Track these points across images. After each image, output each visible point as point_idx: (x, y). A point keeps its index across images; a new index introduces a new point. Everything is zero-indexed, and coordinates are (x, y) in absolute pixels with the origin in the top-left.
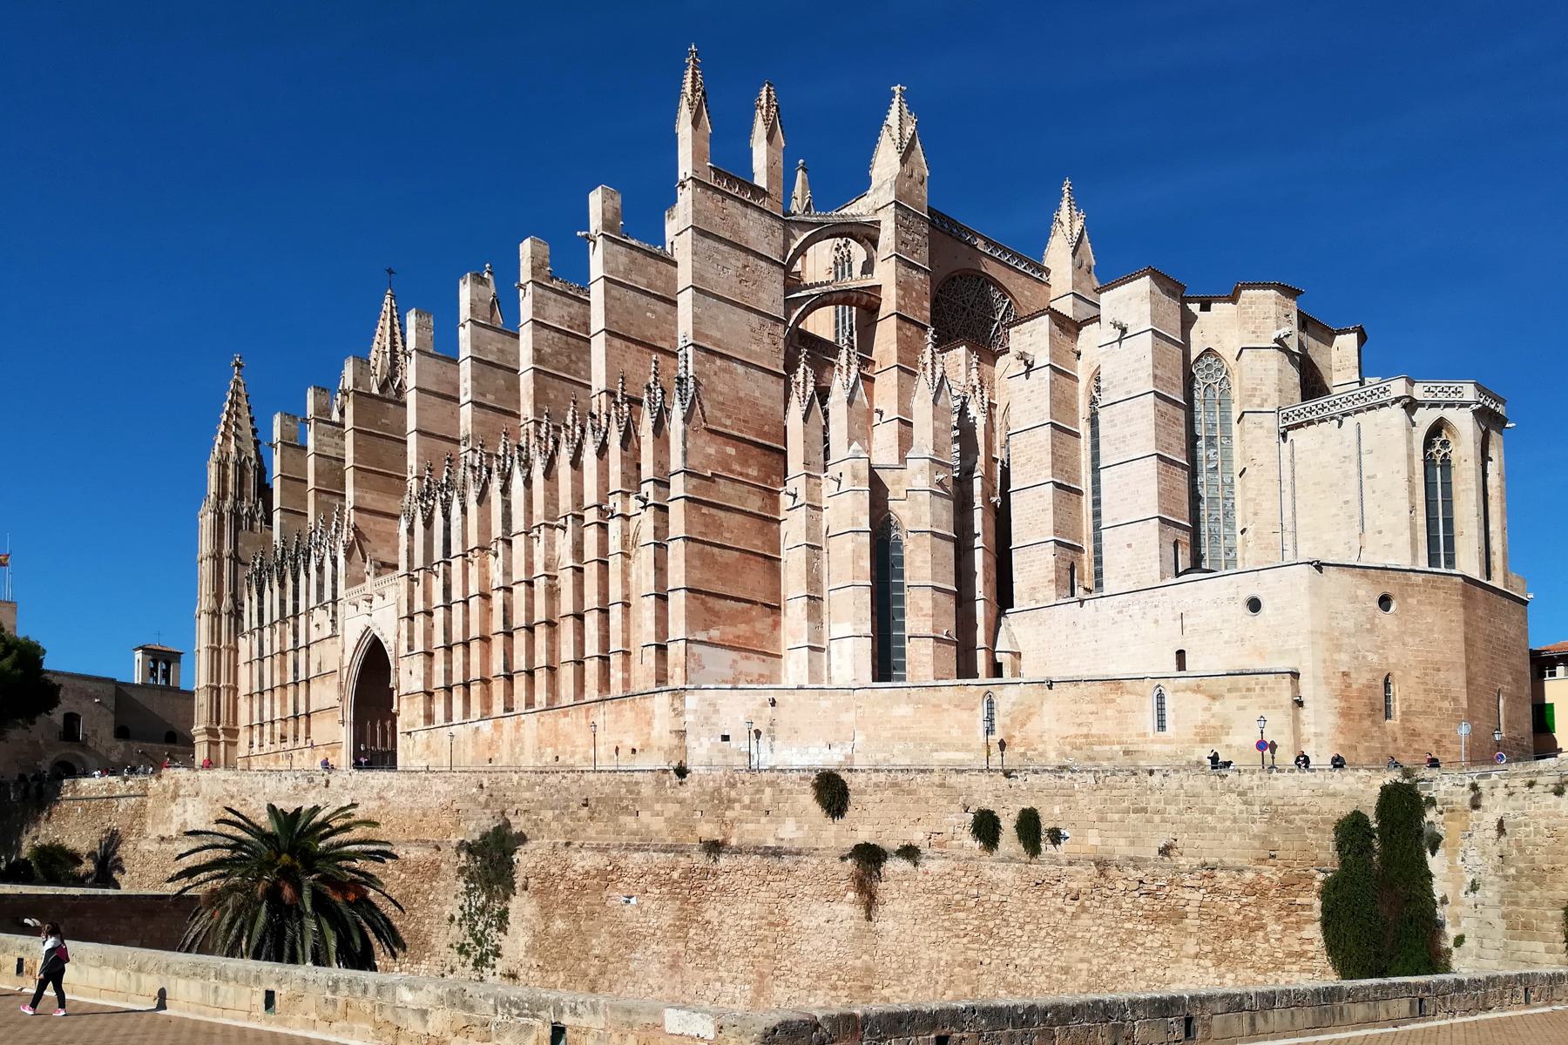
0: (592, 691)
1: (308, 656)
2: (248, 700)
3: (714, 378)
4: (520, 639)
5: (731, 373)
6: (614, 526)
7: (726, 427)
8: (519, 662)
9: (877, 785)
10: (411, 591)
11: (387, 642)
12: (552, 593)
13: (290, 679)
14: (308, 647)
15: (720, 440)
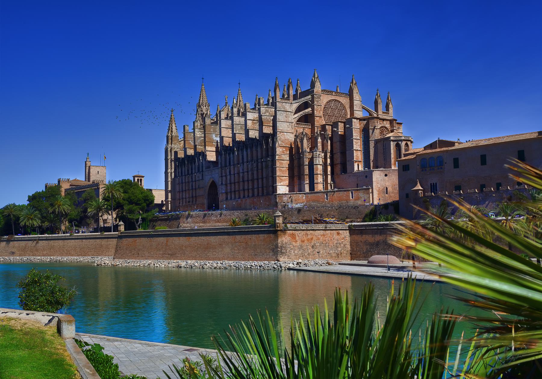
0: (260, 194)
1: (196, 183)
2: (178, 193)
3: (281, 137)
4: (246, 183)
5: (284, 135)
6: (264, 163)
7: (283, 145)
8: (246, 187)
9: (307, 210)
10: (222, 171)
11: (216, 181)
12: (253, 174)
13: (191, 188)
14: (195, 181)
15: (282, 147)
